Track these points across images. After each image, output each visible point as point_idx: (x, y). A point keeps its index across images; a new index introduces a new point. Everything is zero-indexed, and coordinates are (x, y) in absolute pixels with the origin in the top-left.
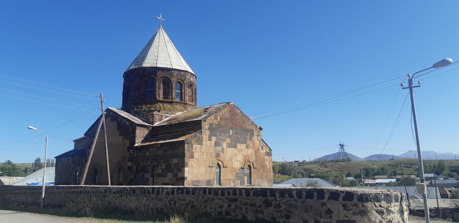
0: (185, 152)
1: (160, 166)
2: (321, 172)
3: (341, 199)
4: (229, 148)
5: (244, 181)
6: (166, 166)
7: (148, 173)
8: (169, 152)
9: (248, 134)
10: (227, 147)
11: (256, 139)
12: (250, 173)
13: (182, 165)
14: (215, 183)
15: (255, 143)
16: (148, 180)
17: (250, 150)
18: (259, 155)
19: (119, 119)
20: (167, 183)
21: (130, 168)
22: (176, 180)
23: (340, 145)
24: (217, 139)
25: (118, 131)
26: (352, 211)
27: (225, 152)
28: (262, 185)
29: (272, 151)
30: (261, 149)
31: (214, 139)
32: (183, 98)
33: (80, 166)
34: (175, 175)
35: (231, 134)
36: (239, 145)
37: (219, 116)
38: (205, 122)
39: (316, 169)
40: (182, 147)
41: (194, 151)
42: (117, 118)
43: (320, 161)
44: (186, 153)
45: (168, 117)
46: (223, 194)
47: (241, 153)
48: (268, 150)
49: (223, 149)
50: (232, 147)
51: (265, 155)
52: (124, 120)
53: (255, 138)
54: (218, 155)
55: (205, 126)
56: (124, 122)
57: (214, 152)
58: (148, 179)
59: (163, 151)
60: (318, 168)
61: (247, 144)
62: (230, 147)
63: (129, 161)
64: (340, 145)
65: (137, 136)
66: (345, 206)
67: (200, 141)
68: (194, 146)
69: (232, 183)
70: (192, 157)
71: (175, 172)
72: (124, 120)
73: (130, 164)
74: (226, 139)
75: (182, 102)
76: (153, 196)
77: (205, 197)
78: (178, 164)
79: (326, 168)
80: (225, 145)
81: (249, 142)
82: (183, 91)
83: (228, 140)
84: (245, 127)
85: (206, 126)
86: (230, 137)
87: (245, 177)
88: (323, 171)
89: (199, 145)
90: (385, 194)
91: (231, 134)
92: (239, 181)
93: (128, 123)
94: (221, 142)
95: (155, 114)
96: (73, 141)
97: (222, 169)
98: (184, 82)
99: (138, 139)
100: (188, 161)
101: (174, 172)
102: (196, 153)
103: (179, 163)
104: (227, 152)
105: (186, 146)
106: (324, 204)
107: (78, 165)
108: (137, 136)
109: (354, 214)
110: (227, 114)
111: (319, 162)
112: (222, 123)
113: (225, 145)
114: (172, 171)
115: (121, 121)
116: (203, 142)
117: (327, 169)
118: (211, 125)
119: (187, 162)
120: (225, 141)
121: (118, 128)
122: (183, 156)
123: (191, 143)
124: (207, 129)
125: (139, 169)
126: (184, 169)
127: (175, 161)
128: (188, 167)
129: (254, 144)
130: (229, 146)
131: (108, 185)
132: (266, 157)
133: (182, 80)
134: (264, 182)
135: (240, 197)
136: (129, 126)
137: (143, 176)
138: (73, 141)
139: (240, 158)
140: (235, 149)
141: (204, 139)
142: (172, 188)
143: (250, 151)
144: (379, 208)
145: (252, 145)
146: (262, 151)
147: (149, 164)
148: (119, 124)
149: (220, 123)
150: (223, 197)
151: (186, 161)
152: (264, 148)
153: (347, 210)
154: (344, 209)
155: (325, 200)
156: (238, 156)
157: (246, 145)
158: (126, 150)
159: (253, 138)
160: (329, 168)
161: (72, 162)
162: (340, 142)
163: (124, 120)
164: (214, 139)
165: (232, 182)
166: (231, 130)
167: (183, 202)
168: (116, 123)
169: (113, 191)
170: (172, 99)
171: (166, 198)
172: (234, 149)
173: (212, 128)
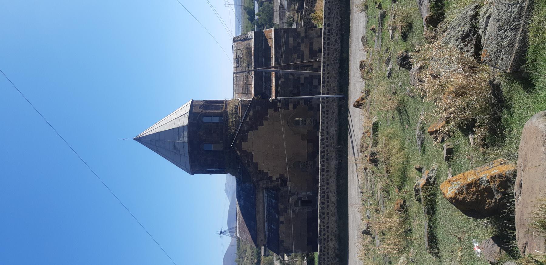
2: (252, 256)
20: (309, 51)
22: (307, 39)
23: (220, 234)
25: (257, 129)
39: (248, 262)
43: (238, 260)
60: (246, 259)
63: (288, 109)
64: (220, 234)
79: (246, 250)
88: (251, 253)
101: (300, 42)
103: (293, 35)
111: (239, 261)
114: (299, 45)
117: (248, 249)
137: (302, 84)
160: (247, 247)
161: (285, 214)
162: (217, 234)
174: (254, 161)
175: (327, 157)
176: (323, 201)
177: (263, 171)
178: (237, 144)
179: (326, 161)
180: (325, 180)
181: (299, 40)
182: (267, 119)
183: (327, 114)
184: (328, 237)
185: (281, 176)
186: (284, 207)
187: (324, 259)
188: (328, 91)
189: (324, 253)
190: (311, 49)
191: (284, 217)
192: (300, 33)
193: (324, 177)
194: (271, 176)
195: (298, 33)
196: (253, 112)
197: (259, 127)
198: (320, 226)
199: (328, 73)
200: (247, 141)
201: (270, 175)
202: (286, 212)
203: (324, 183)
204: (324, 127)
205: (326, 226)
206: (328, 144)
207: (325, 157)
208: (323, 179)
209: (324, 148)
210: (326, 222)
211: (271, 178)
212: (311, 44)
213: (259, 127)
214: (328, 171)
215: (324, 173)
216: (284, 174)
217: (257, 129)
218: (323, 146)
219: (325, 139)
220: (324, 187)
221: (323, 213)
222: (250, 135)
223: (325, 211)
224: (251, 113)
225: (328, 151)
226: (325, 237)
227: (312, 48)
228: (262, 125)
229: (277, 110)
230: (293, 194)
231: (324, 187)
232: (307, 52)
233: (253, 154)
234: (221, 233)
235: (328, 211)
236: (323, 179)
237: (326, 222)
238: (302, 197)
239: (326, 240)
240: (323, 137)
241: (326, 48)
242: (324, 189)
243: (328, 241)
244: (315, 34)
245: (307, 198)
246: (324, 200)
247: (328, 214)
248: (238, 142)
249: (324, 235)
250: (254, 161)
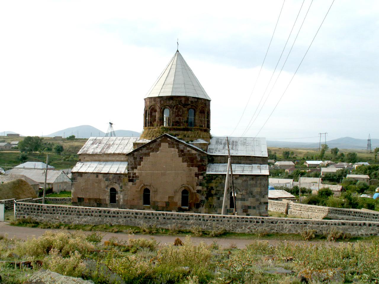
23: (110, 123)
25: (179, 157)
56: (188, 151)
59: (243, 181)
63: (197, 185)
64: (110, 123)
78: (261, 192)
107: (116, 183)
114: (254, 197)
136: (197, 155)
161: (105, 180)
168: (177, 150)
174: (151, 153)
175: (148, 218)
176: (110, 213)
177: (142, 161)
178: (167, 139)
179: (145, 216)
180: (128, 215)
181: (258, 197)
182: (188, 166)
183: (185, 219)
184: (80, 215)
185: (137, 177)
186: (110, 178)
187: (62, 211)
188: (206, 220)
189: (68, 211)
190: (249, 207)
191: (102, 178)
192: (264, 197)
193: (131, 214)
194: (138, 168)
195: (264, 196)
196: (195, 154)
197: (181, 159)
198: (90, 209)
199: (221, 220)
200: (169, 147)
201: (138, 167)
202: (106, 180)
203: (126, 214)
204: (175, 216)
205: (90, 214)
206: (160, 218)
207: (148, 216)
208: (129, 213)
209: (156, 215)
210: (93, 214)
211: (136, 168)
212: (254, 208)
213: (181, 159)
214: (136, 218)
215: (134, 214)
216: (138, 180)
217: (179, 157)
218: (158, 215)
219: (164, 216)
220: (122, 213)
221: (100, 212)
222: (174, 151)
223: (102, 213)
224: (194, 152)
225: (153, 219)
226: (81, 212)
227: (250, 208)
228: (183, 162)
229: (197, 175)
230: (121, 187)
231: (122, 213)
232: (247, 203)
233: (157, 153)
234: (111, 124)
235: (102, 216)
236: (129, 213)
237: (93, 214)
238: (119, 195)
239: (78, 213)
240: (165, 215)
241: (243, 219)
242: (121, 213)
243: (77, 215)
244: (262, 211)
245: (118, 199)
246: (111, 213)
247: (100, 216)
248: (168, 139)
249: (83, 212)
250: (151, 153)
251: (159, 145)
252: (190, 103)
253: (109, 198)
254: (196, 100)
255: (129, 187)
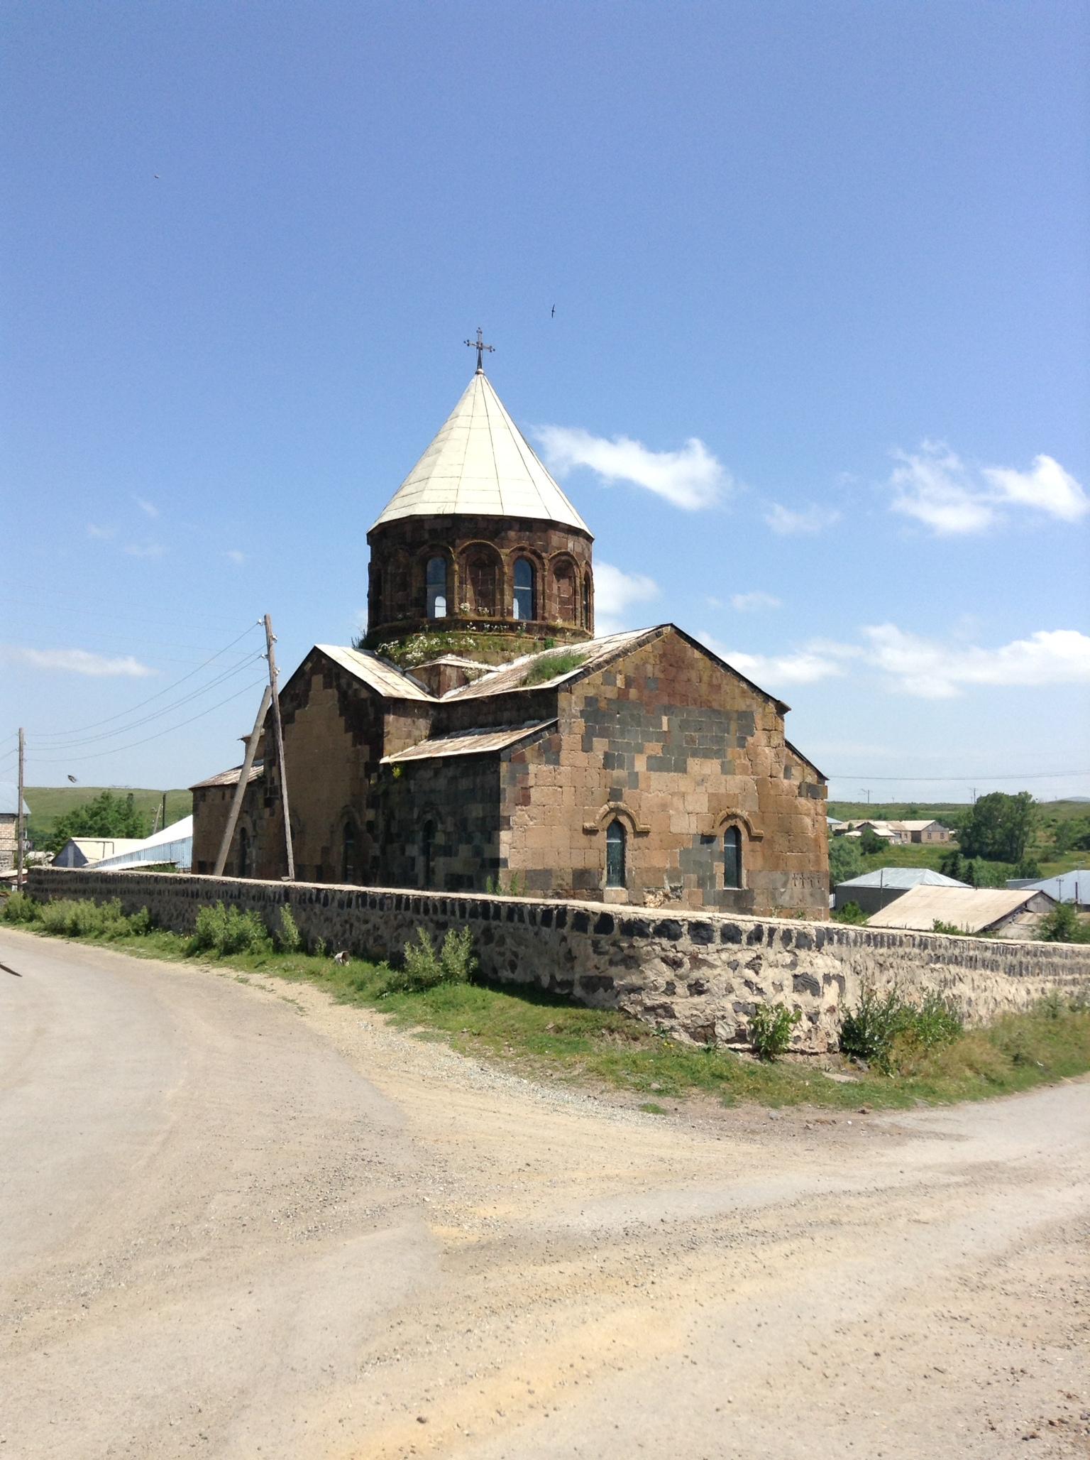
0: (502, 786)
1: (442, 823)
3: (591, 928)
4: (658, 773)
5: (712, 878)
6: (455, 825)
7: (413, 842)
8: (464, 784)
9: (728, 724)
10: (649, 769)
11: (764, 741)
12: (738, 850)
13: (493, 824)
14: (605, 879)
15: (757, 755)
16: (413, 865)
17: (738, 777)
18: (772, 792)
19: (343, 681)
21: (371, 826)
24: (612, 743)
26: (607, 957)
27: (642, 785)
28: (783, 890)
29: (826, 781)
30: (782, 775)
31: (600, 745)
32: (540, 611)
33: (252, 817)
34: (478, 852)
35: (665, 728)
36: (694, 765)
37: (620, 672)
38: (571, 693)
40: (492, 770)
41: (531, 782)
42: (338, 676)
44: (504, 789)
45: (489, 671)
46: (426, 912)
47: (701, 789)
48: (811, 779)
49: (634, 776)
50: (668, 770)
51: (800, 795)
52: (354, 683)
53: (759, 737)
54: (615, 795)
55: (570, 705)
57: (603, 784)
58: (413, 859)
61: (725, 757)
62: (660, 769)
63: (367, 807)
65: (388, 733)
66: (596, 945)
67: (552, 754)
68: (532, 768)
69: (666, 882)
70: (525, 800)
71: (477, 842)
72: (356, 685)
73: (370, 814)
74: (647, 744)
75: (534, 622)
76: (318, 908)
77: (400, 917)
80: (640, 764)
81: (732, 752)
82: (540, 587)
83: (655, 748)
84: (721, 705)
85: (573, 705)
86: (662, 737)
87: (715, 863)
89: (546, 763)
90: (690, 924)
91: (665, 728)
92: (694, 877)
93: (364, 694)
94: (625, 754)
95: (446, 665)
96: (242, 739)
97: (630, 838)
98: (540, 558)
99: (390, 741)
100: (510, 814)
102: (539, 789)
104: (649, 786)
105: (504, 767)
106: (564, 939)
108: (388, 733)
109: (611, 963)
110: (649, 668)
112: (633, 693)
113: (640, 764)
114: (469, 840)
115: (349, 685)
116: (563, 754)
118: (590, 701)
119: (505, 814)
120: (641, 751)
121: (340, 709)
122: (494, 797)
123: (522, 760)
124: (575, 717)
125: (394, 830)
126: (499, 836)
127: (476, 811)
128: (510, 828)
129: (752, 756)
130: (657, 765)
131: (281, 872)
132: (802, 801)
133: (534, 552)
134: (791, 882)
135: (452, 918)
136: (369, 702)
137: (403, 851)
138: (242, 739)
139: (700, 803)
140: (680, 774)
141: (565, 745)
142: (350, 892)
143: (735, 783)
144: (671, 955)
145: (747, 762)
146: (786, 781)
147: (415, 816)
148: (343, 696)
149: (623, 694)
150: (427, 918)
151: (504, 813)
152: (796, 771)
153: (600, 953)
154: (595, 952)
155: (565, 931)
156: (689, 798)
157: (723, 762)
158: (362, 773)
159: (749, 738)
163: (356, 685)
164: (600, 745)
165: (665, 877)
166: (666, 715)
167: (364, 927)
169: (253, 892)
170: (502, 615)
171: (338, 915)
172: (676, 774)
173: (594, 713)
174: (297, 711)
195: (490, 833)
251: (309, 683)
252: (426, 536)
253: (238, 861)
254: (448, 524)
255: (265, 823)
